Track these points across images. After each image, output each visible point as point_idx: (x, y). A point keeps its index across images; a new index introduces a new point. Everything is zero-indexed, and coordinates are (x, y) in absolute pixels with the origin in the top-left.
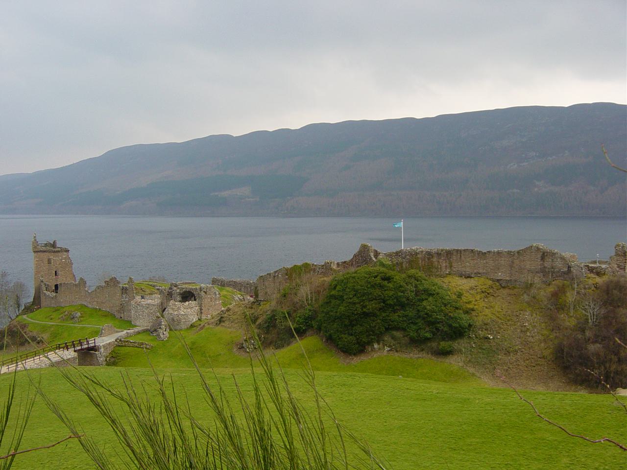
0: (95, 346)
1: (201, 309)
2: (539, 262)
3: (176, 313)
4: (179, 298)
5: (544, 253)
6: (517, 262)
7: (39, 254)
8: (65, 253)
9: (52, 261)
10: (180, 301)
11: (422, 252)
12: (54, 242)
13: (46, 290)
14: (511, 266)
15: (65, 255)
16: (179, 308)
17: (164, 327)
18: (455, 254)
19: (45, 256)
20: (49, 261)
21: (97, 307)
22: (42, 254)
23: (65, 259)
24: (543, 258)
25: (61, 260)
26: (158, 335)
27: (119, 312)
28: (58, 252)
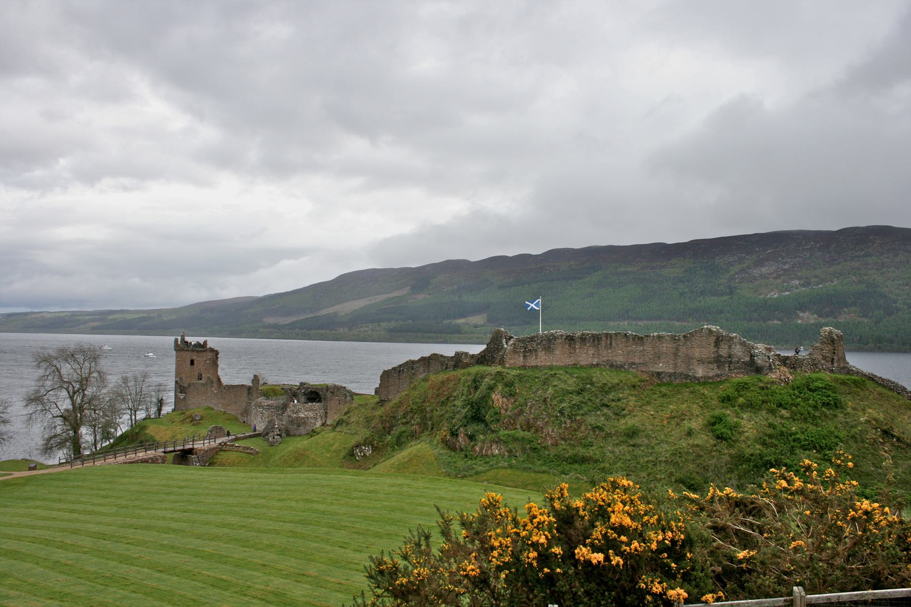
0: (193, 449)
1: (326, 413)
2: (712, 348)
4: (303, 399)
5: (718, 338)
6: (683, 350)
7: (182, 353)
8: (210, 354)
11: (562, 336)
12: (205, 342)
14: (676, 355)
15: (210, 355)
18: (604, 339)
19: (188, 356)
20: (192, 362)
22: (184, 354)
24: (717, 343)
27: (242, 414)
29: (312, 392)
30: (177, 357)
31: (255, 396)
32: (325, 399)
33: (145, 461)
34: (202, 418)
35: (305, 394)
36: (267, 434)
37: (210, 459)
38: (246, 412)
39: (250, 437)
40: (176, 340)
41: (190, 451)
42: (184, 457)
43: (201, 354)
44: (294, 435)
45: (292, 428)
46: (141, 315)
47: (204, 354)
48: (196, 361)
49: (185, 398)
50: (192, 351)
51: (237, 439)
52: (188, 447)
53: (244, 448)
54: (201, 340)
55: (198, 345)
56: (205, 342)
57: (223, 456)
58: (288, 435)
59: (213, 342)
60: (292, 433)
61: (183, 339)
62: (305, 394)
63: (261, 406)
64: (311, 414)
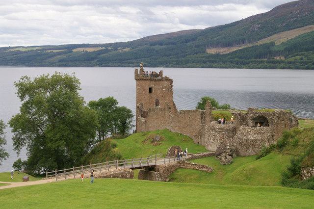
0: (155, 166)
3: (244, 138)
4: (251, 123)
8: (166, 82)
9: (153, 90)
10: (254, 126)
12: (161, 73)
13: (142, 117)
15: (166, 84)
16: (248, 133)
17: (229, 151)
19: (147, 85)
20: (150, 90)
21: (179, 132)
22: (143, 83)
23: (166, 87)
25: (162, 89)
26: (221, 159)
27: (196, 136)
28: (160, 80)
29: (259, 117)
30: (137, 85)
31: (208, 119)
32: (272, 123)
33: (116, 176)
34: (161, 139)
35: (253, 119)
36: (220, 154)
37: (170, 175)
38: (200, 135)
39: (204, 156)
40: (136, 71)
41: (152, 168)
42: (148, 172)
43: (157, 82)
44: (244, 156)
45: (242, 151)
46: (100, 49)
47: (161, 83)
48: (154, 89)
49: (145, 121)
50: (151, 80)
51: (193, 158)
52: (150, 164)
53: (199, 166)
54: (157, 70)
55: (154, 75)
56: (161, 73)
57: (180, 172)
58: (238, 155)
59: (168, 72)
60: (242, 153)
61: (142, 70)
62: (253, 119)
63: (214, 129)
64: (259, 137)
